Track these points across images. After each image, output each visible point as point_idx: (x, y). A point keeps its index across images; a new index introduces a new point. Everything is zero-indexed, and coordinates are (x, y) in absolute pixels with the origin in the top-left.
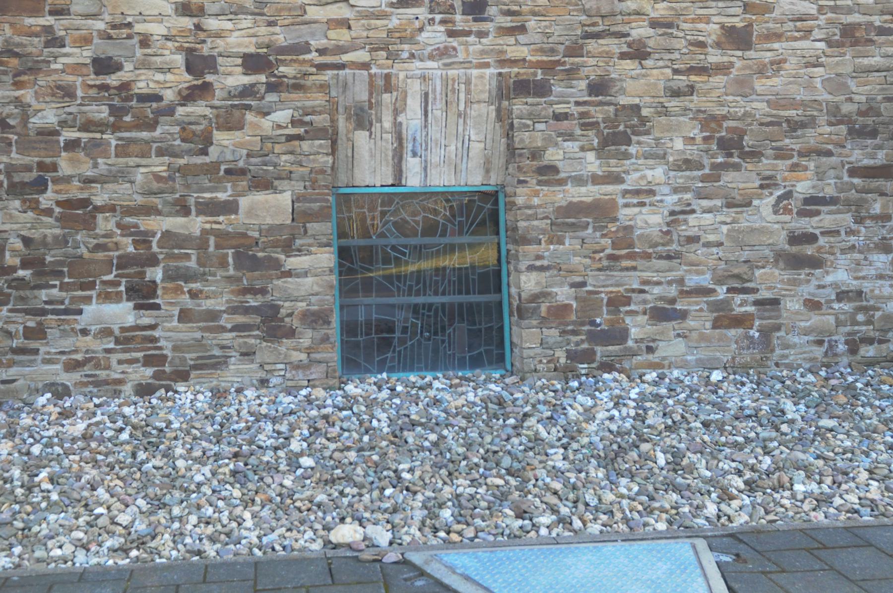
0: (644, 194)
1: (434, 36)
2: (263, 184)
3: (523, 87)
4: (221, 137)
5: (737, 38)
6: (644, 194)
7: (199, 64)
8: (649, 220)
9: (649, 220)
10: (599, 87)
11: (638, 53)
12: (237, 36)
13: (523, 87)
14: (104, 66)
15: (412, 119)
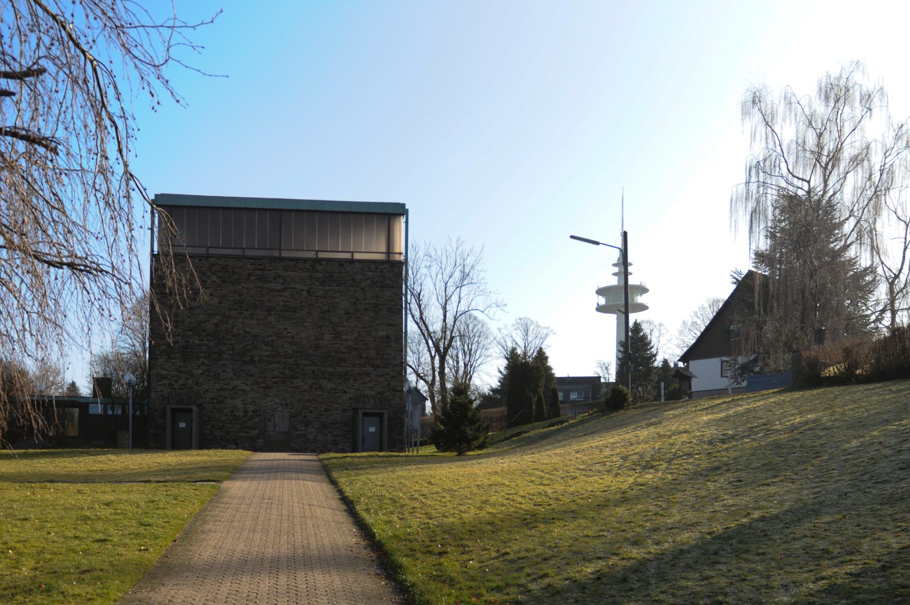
0: (310, 433)
1: (280, 409)
2: (254, 429)
3: (293, 417)
4: (249, 422)
5: (326, 410)
6: (310, 433)
7: (245, 412)
8: (311, 437)
9: (311, 437)
10: (305, 417)
11: (311, 412)
12: (251, 408)
13: (293, 417)
14: (232, 412)
15: (277, 420)
